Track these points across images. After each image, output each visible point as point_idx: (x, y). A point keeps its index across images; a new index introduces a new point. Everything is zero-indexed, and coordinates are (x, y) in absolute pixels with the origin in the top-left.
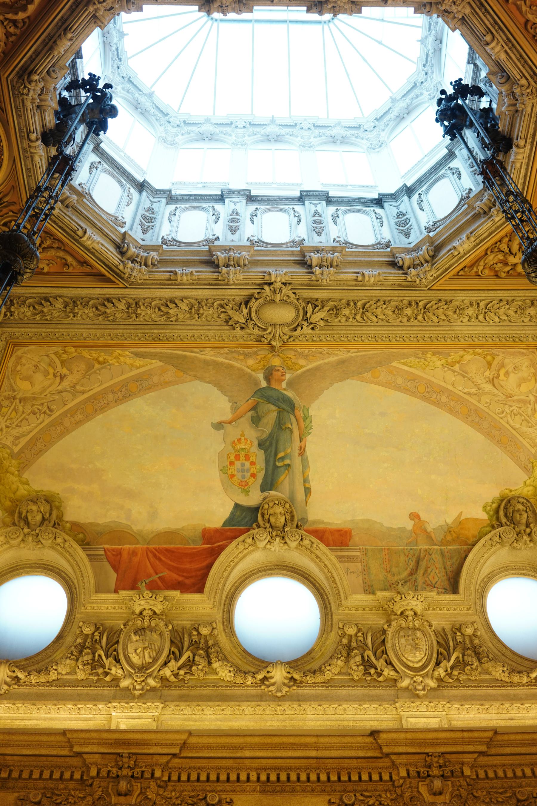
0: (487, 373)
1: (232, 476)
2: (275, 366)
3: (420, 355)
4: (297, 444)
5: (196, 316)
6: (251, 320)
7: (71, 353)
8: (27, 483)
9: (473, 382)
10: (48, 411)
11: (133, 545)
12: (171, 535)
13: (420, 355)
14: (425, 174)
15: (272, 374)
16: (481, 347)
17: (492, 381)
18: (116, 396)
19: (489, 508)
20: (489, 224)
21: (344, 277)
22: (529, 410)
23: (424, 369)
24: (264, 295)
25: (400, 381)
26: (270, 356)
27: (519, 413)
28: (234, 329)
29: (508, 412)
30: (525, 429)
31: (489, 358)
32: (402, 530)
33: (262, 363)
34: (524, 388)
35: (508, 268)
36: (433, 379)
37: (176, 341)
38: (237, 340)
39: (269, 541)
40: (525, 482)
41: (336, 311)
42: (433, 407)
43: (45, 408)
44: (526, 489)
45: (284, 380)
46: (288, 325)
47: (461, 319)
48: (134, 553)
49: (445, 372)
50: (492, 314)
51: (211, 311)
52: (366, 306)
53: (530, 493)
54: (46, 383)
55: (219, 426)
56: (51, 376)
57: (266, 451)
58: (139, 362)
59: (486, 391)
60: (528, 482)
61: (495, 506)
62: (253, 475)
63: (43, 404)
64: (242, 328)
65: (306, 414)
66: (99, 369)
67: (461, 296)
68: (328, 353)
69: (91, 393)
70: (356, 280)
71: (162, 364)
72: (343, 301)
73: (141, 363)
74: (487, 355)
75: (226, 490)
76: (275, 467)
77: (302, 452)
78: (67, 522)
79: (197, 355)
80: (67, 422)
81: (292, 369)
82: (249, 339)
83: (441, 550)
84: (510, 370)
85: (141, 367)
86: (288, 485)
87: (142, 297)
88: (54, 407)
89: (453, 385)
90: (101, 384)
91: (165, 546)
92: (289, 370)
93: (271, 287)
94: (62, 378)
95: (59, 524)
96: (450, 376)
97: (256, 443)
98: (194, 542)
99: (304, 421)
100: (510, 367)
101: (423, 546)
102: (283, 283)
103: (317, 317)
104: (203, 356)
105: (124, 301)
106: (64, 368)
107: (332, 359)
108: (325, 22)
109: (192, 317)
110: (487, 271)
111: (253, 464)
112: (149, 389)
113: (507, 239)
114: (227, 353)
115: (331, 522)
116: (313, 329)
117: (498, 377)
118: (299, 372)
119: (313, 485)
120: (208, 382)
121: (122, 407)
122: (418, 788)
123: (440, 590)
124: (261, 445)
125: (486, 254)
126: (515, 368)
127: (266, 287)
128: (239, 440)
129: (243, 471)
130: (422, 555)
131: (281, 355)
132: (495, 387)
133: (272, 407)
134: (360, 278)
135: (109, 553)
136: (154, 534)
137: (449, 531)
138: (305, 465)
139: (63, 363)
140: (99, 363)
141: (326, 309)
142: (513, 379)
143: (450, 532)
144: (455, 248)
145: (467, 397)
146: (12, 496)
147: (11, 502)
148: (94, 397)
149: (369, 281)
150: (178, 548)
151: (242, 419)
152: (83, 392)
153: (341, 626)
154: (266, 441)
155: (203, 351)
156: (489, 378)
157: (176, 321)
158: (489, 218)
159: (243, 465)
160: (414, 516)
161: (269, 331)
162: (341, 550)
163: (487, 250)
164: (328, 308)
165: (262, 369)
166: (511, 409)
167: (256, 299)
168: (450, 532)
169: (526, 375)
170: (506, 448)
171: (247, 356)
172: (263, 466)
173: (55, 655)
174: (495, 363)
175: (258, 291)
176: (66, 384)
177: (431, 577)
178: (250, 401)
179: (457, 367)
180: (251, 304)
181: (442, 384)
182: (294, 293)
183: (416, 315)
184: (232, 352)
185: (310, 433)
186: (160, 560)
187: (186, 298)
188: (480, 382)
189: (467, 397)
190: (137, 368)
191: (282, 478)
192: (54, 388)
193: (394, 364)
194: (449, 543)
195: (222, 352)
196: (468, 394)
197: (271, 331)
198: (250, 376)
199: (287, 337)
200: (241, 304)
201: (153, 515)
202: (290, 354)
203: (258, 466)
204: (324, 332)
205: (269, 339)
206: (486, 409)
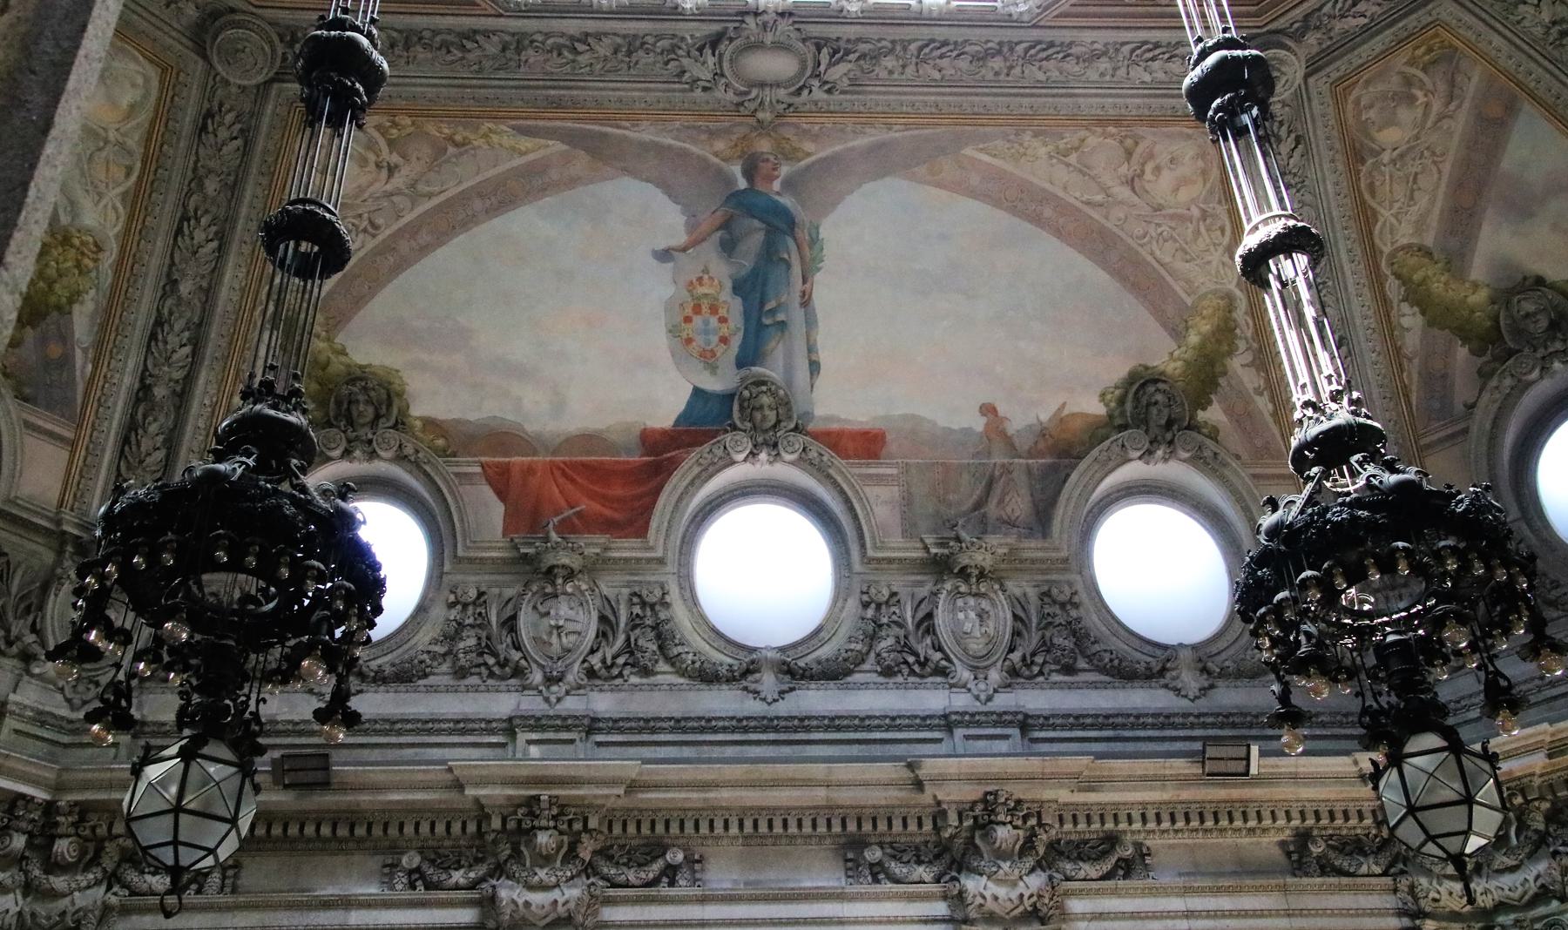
1: (689, 341)
3: (1012, 137)
4: (798, 285)
6: (723, 75)
7: (404, 127)
8: (343, 352)
10: (370, 229)
11: (528, 455)
12: (589, 440)
13: (1012, 137)
15: (756, 167)
16: (1117, 122)
17: (1130, 183)
18: (488, 203)
19: (1109, 397)
22: (1190, 231)
24: (745, 33)
25: (975, 180)
27: (1172, 237)
29: (1154, 234)
30: (1179, 265)
31: (1129, 142)
32: (967, 431)
34: (1184, 195)
39: (751, 453)
40: (1171, 354)
42: (1029, 226)
43: (365, 223)
44: (1172, 365)
48: (530, 470)
49: (1052, 166)
51: (651, 58)
53: (1177, 372)
54: (363, 180)
55: (665, 255)
56: (372, 166)
57: (745, 299)
58: (525, 143)
59: (1120, 198)
60: (1176, 353)
61: (1117, 392)
62: (724, 340)
63: (360, 216)
65: (814, 236)
66: (455, 156)
67: (1088, 36)
68: (854, 132)
69: (442, 198)
71: (565, 147)
73: (529, 145)
74: (1126, 136)
75: (678, 365)
76: (761, 327)
77: (806, 300)
78: (417, 418)
79: (626, 132)
80: (404, 246)
81: (791, 159)
83: (1027, 464)
86: (781, 356)
88: (380, 221)
89: (1065, 188)
90: (460, 182)
91: (579, 458)
92: (787, 159)
94: (392, 170)
95: (403, 423)
96: (1061, 174)
97: (728, 285)
98: (629, 452)
99: (811, 248)
100: (1163, 158)
101: (999, 459)
103: (838, 73)
105: (495, 39)
106: (395, 154)
107: (861, 142)
111: (723, 320)
112: (544, 190)
115: (850, 418)
116: (829, 91)
118: (803, 163)
119: (823, 356)
120: (648, 180)
121: (497, 222)
122: (973, 837)
123: (1023, 531)
124: (738, 289)
126: (1172, 161)
127: (750, 20)
128: (700, 279)
129: (706, 332)
130: (997, 473)
132: (1135, 192)
133: (756, 223)
135: (490, 471)
136: (563, 438)
137: (1043, 433)
138: (811, 322)
139: (391, 143)
140: (457, 145)
142: (1167, 179)
143: (1044, 435)
145: (1086, 209)
146: (320, 373)
147: (320, 384)
148: (449, 203)
150: (602, 463)
151: (704, 244)
152: (430, 196)
153: (865, 589)
154: (745, 281)
156: (1126, 176)
157: (591, 73)
159: (706, 323)
160: (988, 410)
161: (753, 95)
162: (868, 465)
165: (740, 157)
166: (1159, 230)
167: (731, 40)
168: (1044, 435)
170: (1145, 296)
171: (713, 134)
172: (741, 325)
173: (416, 638)
174: (1139, 149)
175: (737, 25)
176: (398, 181)
177: (1009, 510)
178: (718, 213)
179: (1073, 159)
180: (722, 47)
181: (1047, 186)
182: (798, 30)
185: (819, 270)
186: (573, 481)
188: (1110, 183)
189: (1086, 209)
190: (522, 154)
191: (773, 344)
192: (378, 188)
193: (968, 151)
194: (1041, 454)
196: (1088, 203)
199: (785, 106)
201: (559, 407)
202: (788, 133)
203: (732, 324)
204: (848, 97)
206: (1115, 230)
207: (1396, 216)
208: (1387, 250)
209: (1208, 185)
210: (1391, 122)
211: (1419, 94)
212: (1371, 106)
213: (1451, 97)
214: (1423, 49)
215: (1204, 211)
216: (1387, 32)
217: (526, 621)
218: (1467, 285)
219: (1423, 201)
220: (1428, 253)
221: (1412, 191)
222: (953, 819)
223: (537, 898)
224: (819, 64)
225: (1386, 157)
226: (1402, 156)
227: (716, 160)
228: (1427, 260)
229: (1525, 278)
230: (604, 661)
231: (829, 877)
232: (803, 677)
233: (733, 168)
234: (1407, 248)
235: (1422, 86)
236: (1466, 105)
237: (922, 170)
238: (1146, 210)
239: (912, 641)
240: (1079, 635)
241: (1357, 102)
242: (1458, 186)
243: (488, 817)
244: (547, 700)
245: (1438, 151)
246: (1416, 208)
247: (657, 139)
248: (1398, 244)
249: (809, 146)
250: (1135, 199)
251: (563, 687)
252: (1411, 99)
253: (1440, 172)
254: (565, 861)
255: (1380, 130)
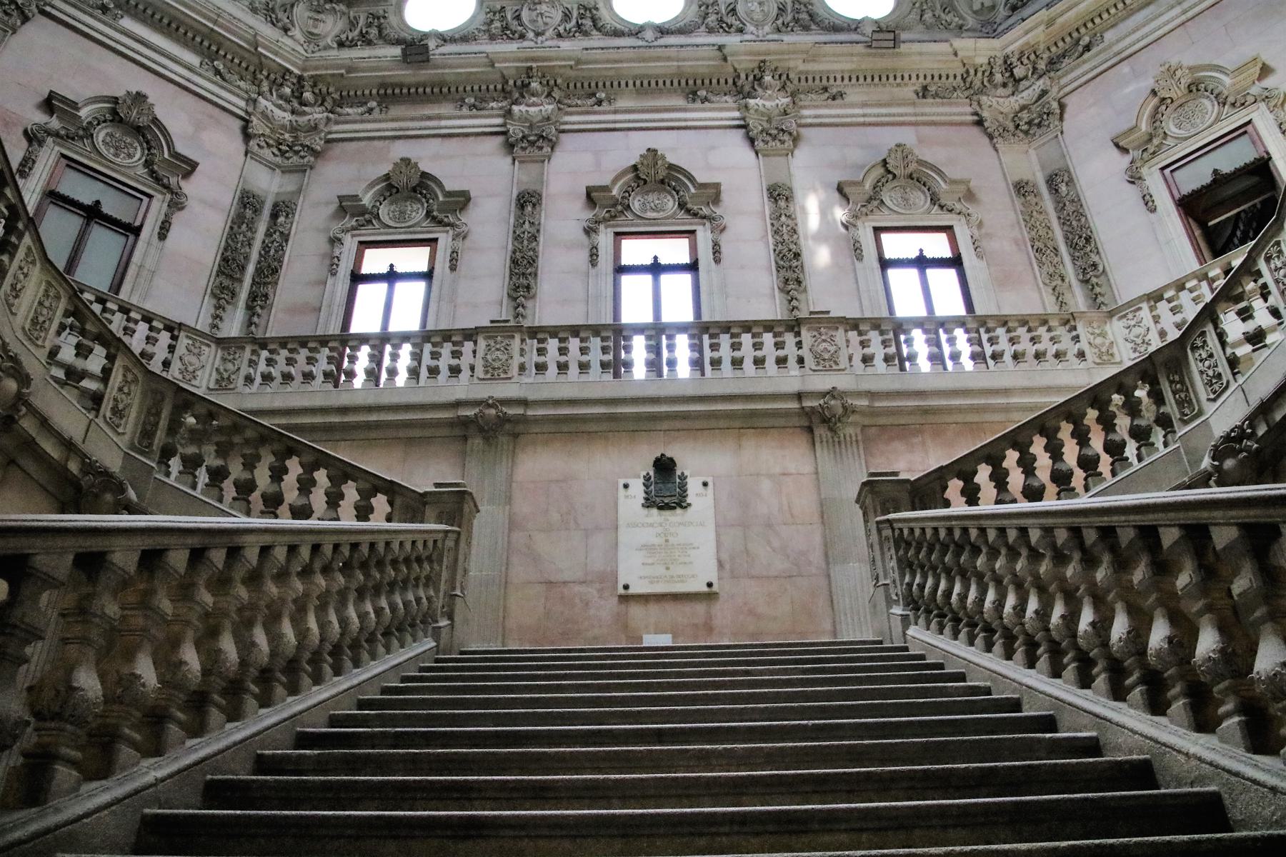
217: (525, 15)
222: (743, 76)
223: (532, 110)
230: (565, 30)
231: (680, 102)
232: (668, 33)
239: (725, 19)
240: (812, 16)
243: (507, 82)
244: (536, 43)
251: (544, 37)
254: (547, 97)
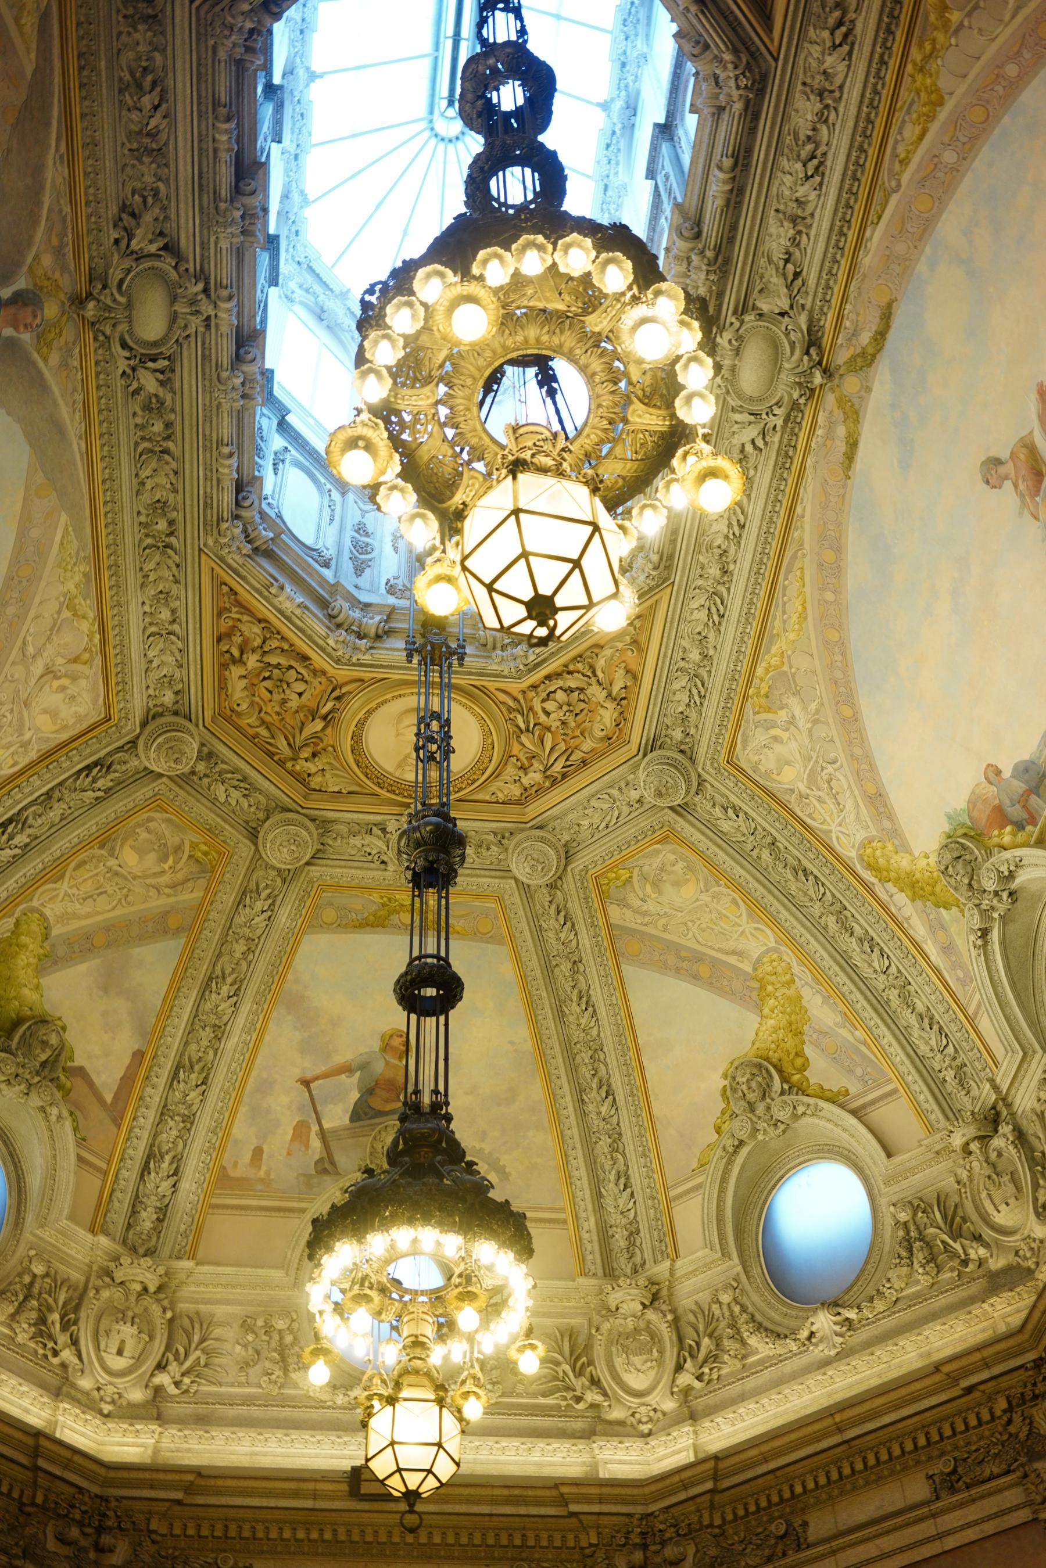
0: (60, 661)
2: (42, 309)
3: (82, 554)
5: (135, 146)
9: (44, 645)
14: (307, 443)
15: (25, 305)
16: (104, 642)
17: (49, 671)
20: (322, 630)
21: (225, 423)
22: (9, 739)
23: (59, 566)
26: (62, 296)
28: (115, 226)
31: (86, 656)
33: (46, 283)
34: (43, 721)
35: (236, 653)
36: (43, 583)
37: (81, 103)
38: (89, 231)
41: (153, 407)
45: (17, 329)
46: (130, 332)
47: (147, 602)
49: (57, 599)
50: (161, 646)
51: (149, 179)
52: (166, 456)
58: (30, 22)
64: (117, 242)
70: (220, 443)
72: (173, 416)
73: (28, 29)
74: (91, 651)
79: (53, 150)
81: (39, 342)
82: (95, 254)
84: (69, 691)
85: (20, 27)
87: (169, 29)
89: (37, 617)
92: (39, 337)
93: (200, 296)
96: (52, 607)
100: (73, 690)
102: (208, 318)
104: (50, 162)
107: (64, 412)
108: (431, 121)
109: (130, 135)
110: (231, 623)
113: (286, 647)
114: (60, 211)
117: (56, 678)
118: (36, 356)
125: (260, 621)
126: (73, 697)
127: (200, 286)
131: (65, 317)
134: (226, 450)
141: (161, 392)
144: (282, 588)
145: (19, 642)
149: (223, 465)
155: (62, 162)
158: (328, 628)
163: (266, 621)
164: (161, 394)
165: (35, 285)
167: (176, 267)
169: (63, 715)
171: (58, 252)
175: (192, 270)
179: (66, 614)
181: (37, 600)
183: (154, 536)
184: (64, 220)
187: (169, 125)
188: (45, 655)
190: (17, 20)
193: (64, 517)
195: (62, 201)
196: (24, 643)
197: (119, 303)
198: (19, 264)
199: (108, 332)
200: (161, 234)
205: (102, 298)
207: (66, 894)
208: (35, 903)
209: (53, 736)
210: (141, 852)
211: (170, 862)
212: (149, 831)
213: (173, 886)
214: (205, 848)
215: (29, 742)
216: (219, 820)
218: (35, 981)
219: (86, 909)
220: (46, 937)
221: (91, 897)
224: (154, 360)
225: (112, 862)
226: (117, 874)
227: (29, 259)
228: (40, 938)
229: (60, 1019)
233: (23, 280)
234: (43, 917)
235: (176, 862)
236: (173, 899)
237: (40, 478)
238: (24, 695)
241: (150, 820)
242: (108, 928)
245: (130, 898)
246: (78, 906)
247: (48, 186)
248: (44, 910)
249: (55, 358)
250: (33, 681)
252: (164, 859)
253: (114, 908)
255: (132, 847)
